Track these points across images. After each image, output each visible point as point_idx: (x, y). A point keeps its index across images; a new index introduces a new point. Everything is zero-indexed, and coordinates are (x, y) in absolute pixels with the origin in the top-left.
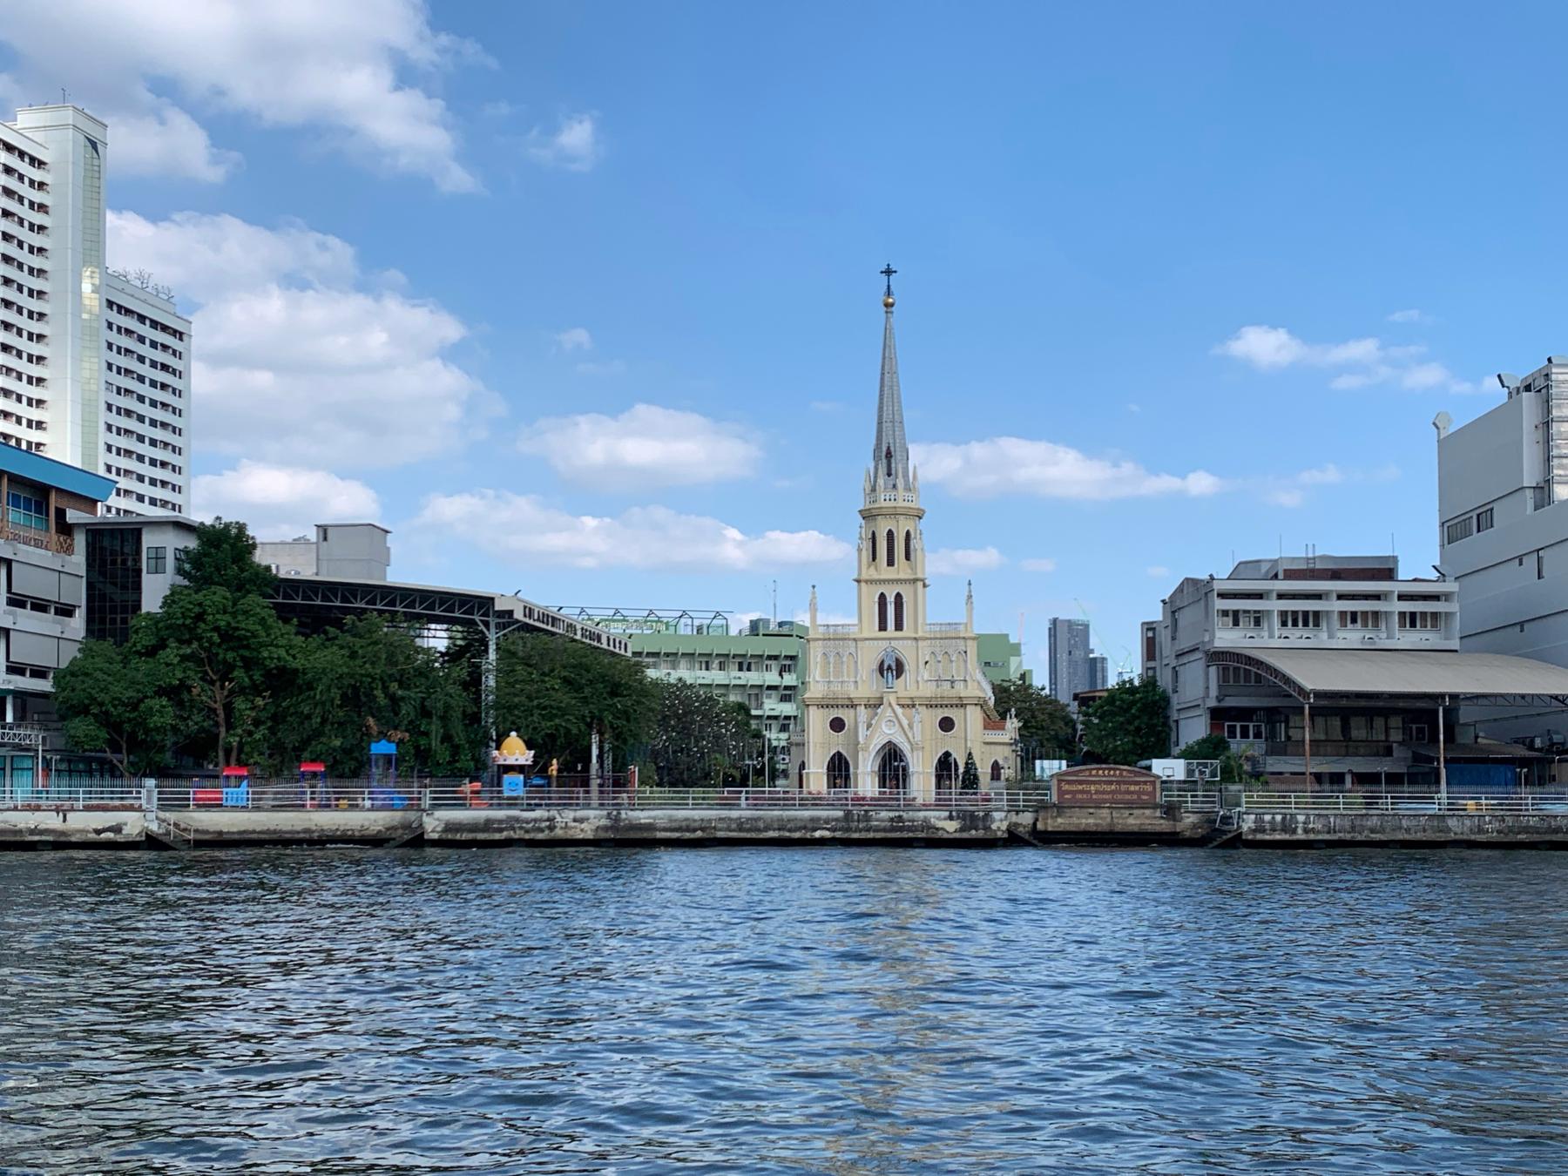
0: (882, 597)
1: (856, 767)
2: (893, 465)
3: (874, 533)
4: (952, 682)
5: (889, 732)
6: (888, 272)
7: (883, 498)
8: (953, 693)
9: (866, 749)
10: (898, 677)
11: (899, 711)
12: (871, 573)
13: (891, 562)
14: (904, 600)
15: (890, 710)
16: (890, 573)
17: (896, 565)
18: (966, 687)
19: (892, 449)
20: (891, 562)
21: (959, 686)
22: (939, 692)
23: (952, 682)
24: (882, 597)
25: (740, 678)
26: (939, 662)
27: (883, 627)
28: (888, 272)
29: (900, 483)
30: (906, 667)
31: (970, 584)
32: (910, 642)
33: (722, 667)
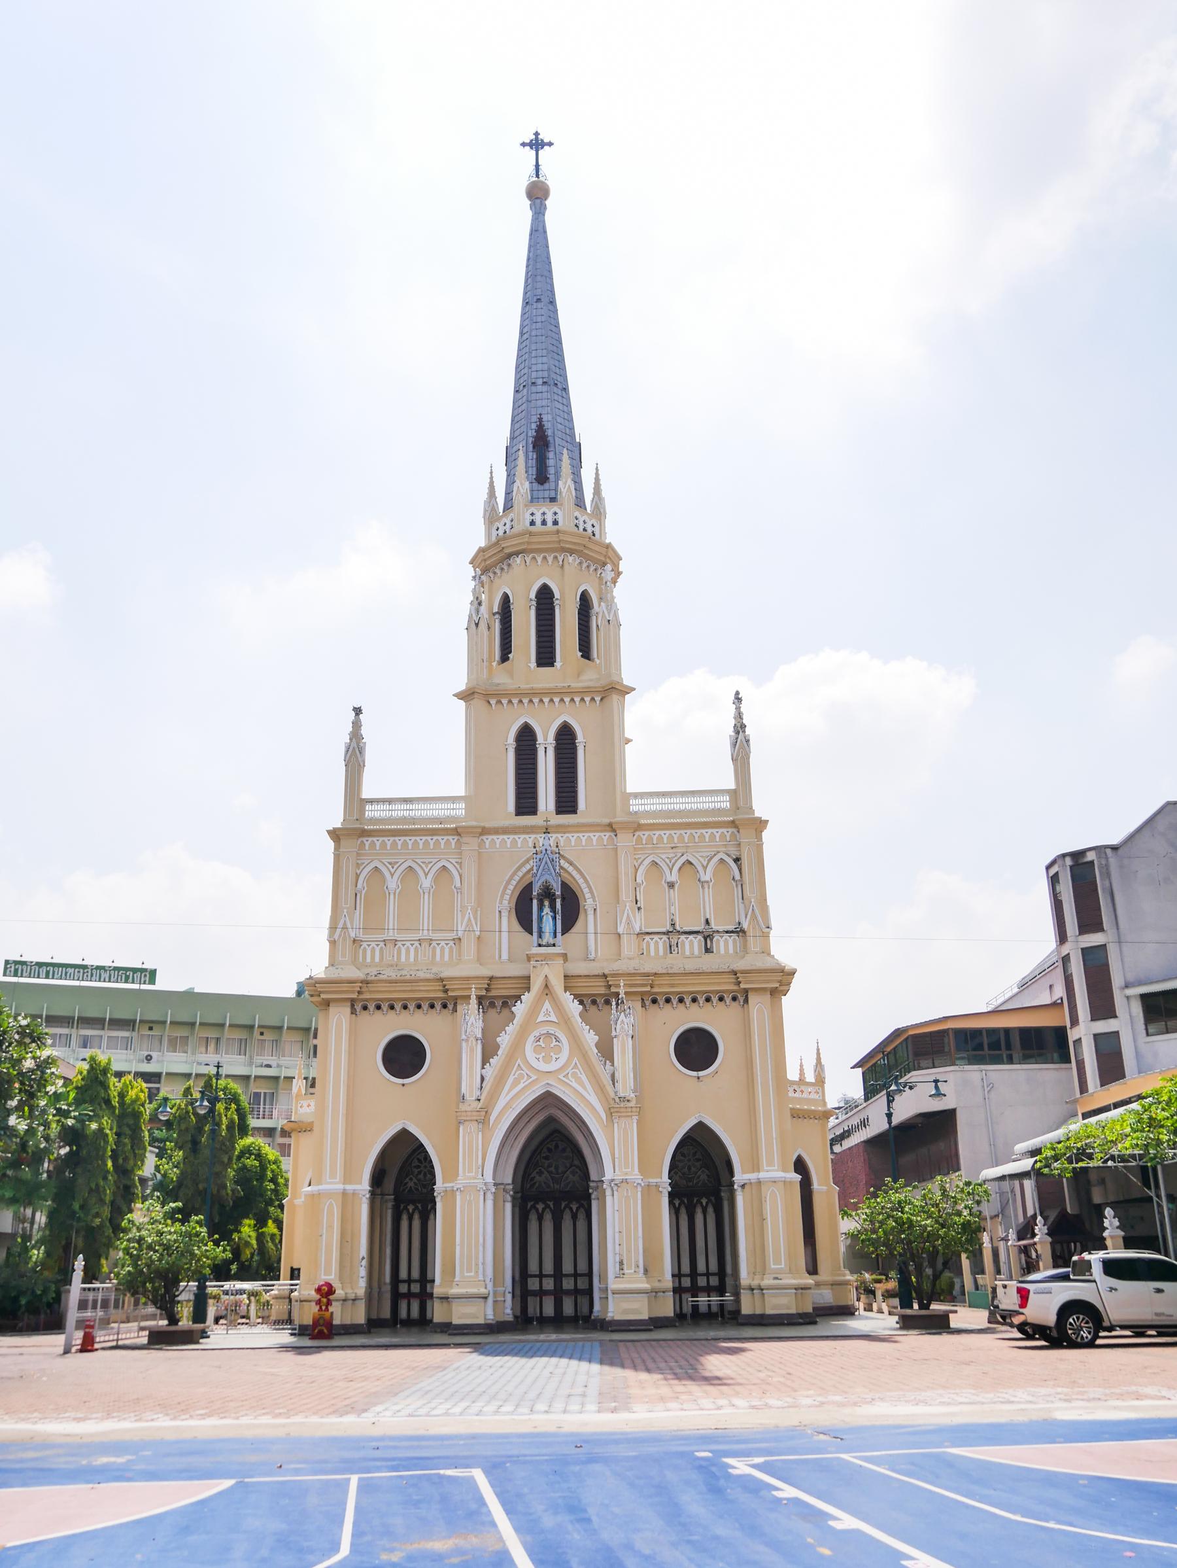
0: (526, 739)
1: (452, 1174)
2: (551, 462)
3: (506, 600)
4: (708, 937)
5: (543, 1067)
6: (537, 144)
7: (528, 518)
8: (708, 963)
9: (483, 1119)
10: (566, 930)
11: (575, 1008)
12: (502, 678)
13: (546, 656)
14: (580, 738)
15: (547, 1005)
16: (546, 677)
17: (558, 664)
18: (745, 948)
19: (547, 425)
20: (546, 656)
21: (725, 945)
22: (676, 963)
23: (708, 937)
24: (526, 737)
25: (269, 1066)
26: (671, 885)
27: (526, 803)
28: (537, 144)
29: (565, 486)
30: (588, 902)
31: (738, 699)
32: (594, 837)
33: (242, 1047)
